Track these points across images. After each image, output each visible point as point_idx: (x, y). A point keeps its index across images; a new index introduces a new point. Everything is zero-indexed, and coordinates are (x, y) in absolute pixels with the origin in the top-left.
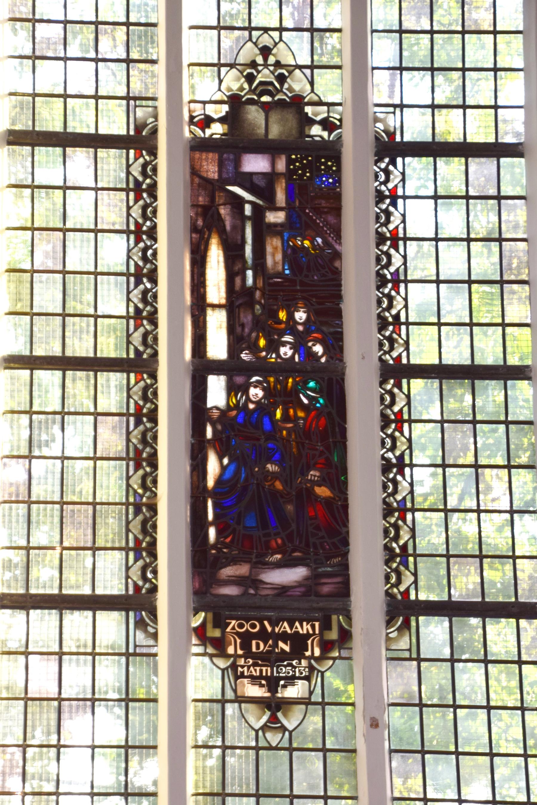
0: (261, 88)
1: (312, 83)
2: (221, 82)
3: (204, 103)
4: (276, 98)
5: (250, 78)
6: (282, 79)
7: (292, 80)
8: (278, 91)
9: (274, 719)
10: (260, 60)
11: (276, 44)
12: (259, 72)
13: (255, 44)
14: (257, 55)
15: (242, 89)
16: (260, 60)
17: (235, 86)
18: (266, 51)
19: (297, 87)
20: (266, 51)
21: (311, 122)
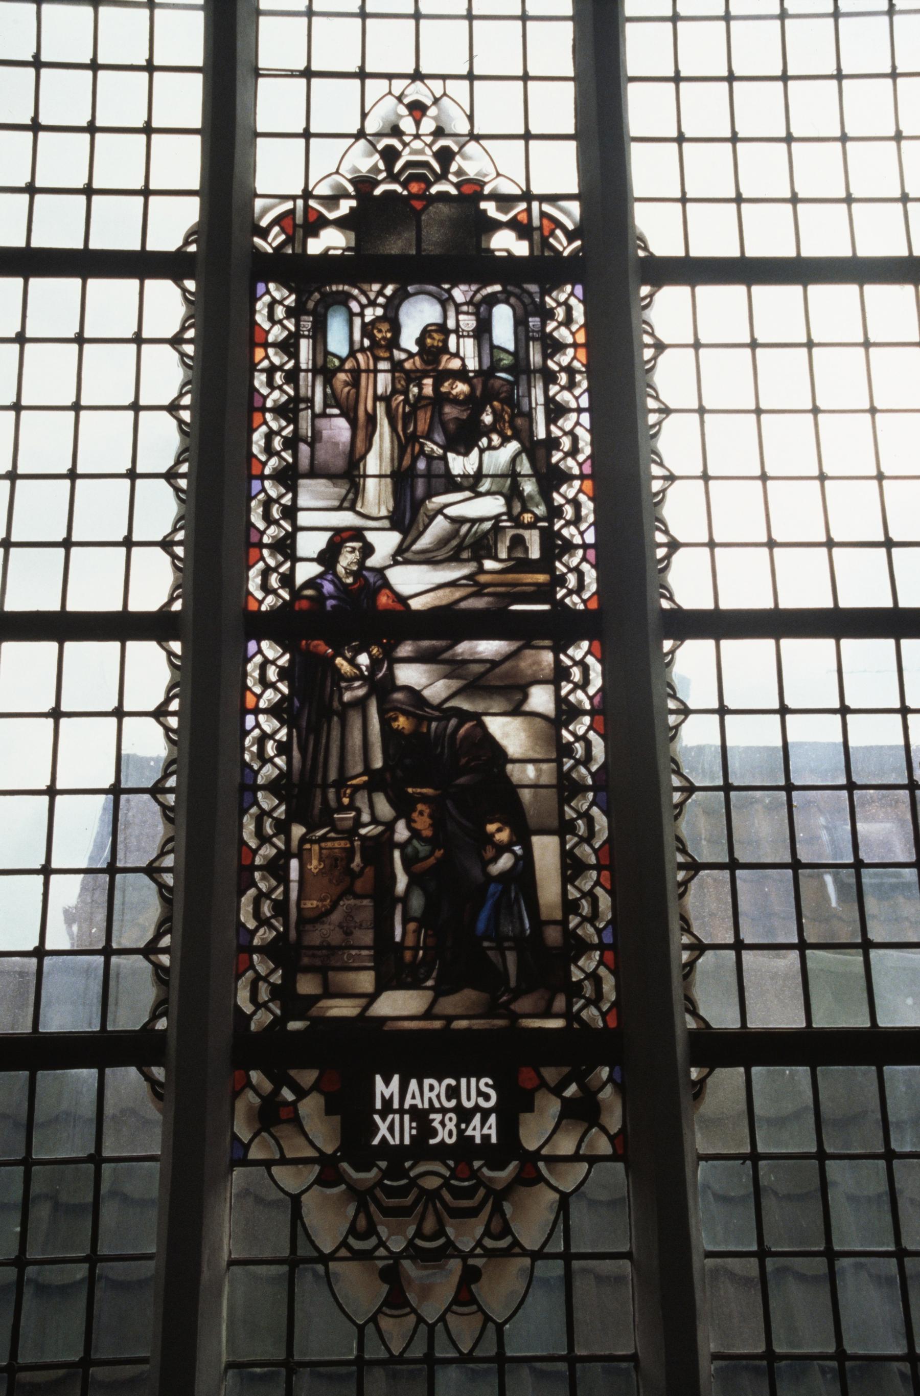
4: (434, 190)
5: (390, 155)
6: (445, 156)
13: (399, 99)
16: (407, 125)
18: (417, 109)
21: (497, 225)
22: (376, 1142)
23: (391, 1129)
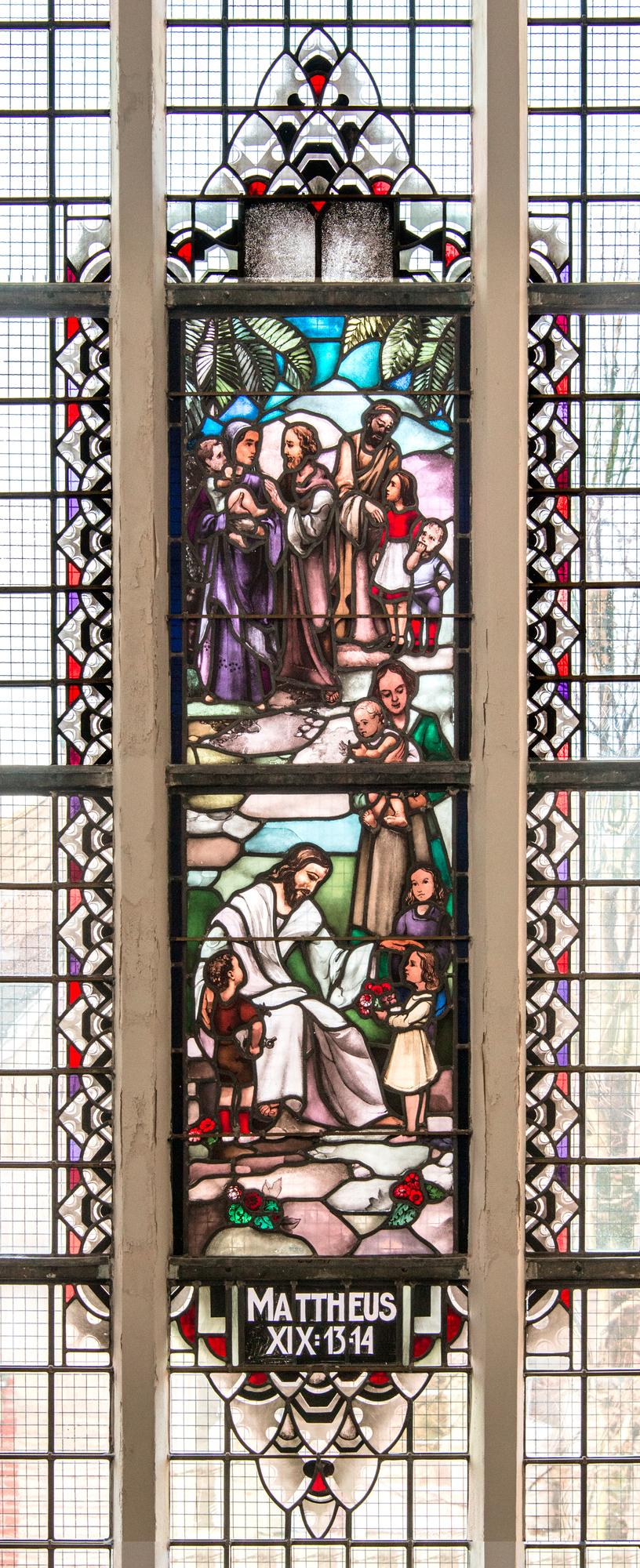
0: (309, 157)
1: (411, 148)
2: (227, 146)
3: (193, 200)
5: (287, 136)
6: (350, 136)
7: (368, 139)
8: (342, 166)
9: (319, 1489)
10: (305, 94)
11: (341, 57)
12: (306, 121)
13: (296, 58)
14: (301, 83)
15: (268, 162)
16: (305, 94)
17: (255, 155)
18: (318, 71)
19: (380, 153)
20: (318, 71)
22: (270, 1351)
23: (284, 1340)
